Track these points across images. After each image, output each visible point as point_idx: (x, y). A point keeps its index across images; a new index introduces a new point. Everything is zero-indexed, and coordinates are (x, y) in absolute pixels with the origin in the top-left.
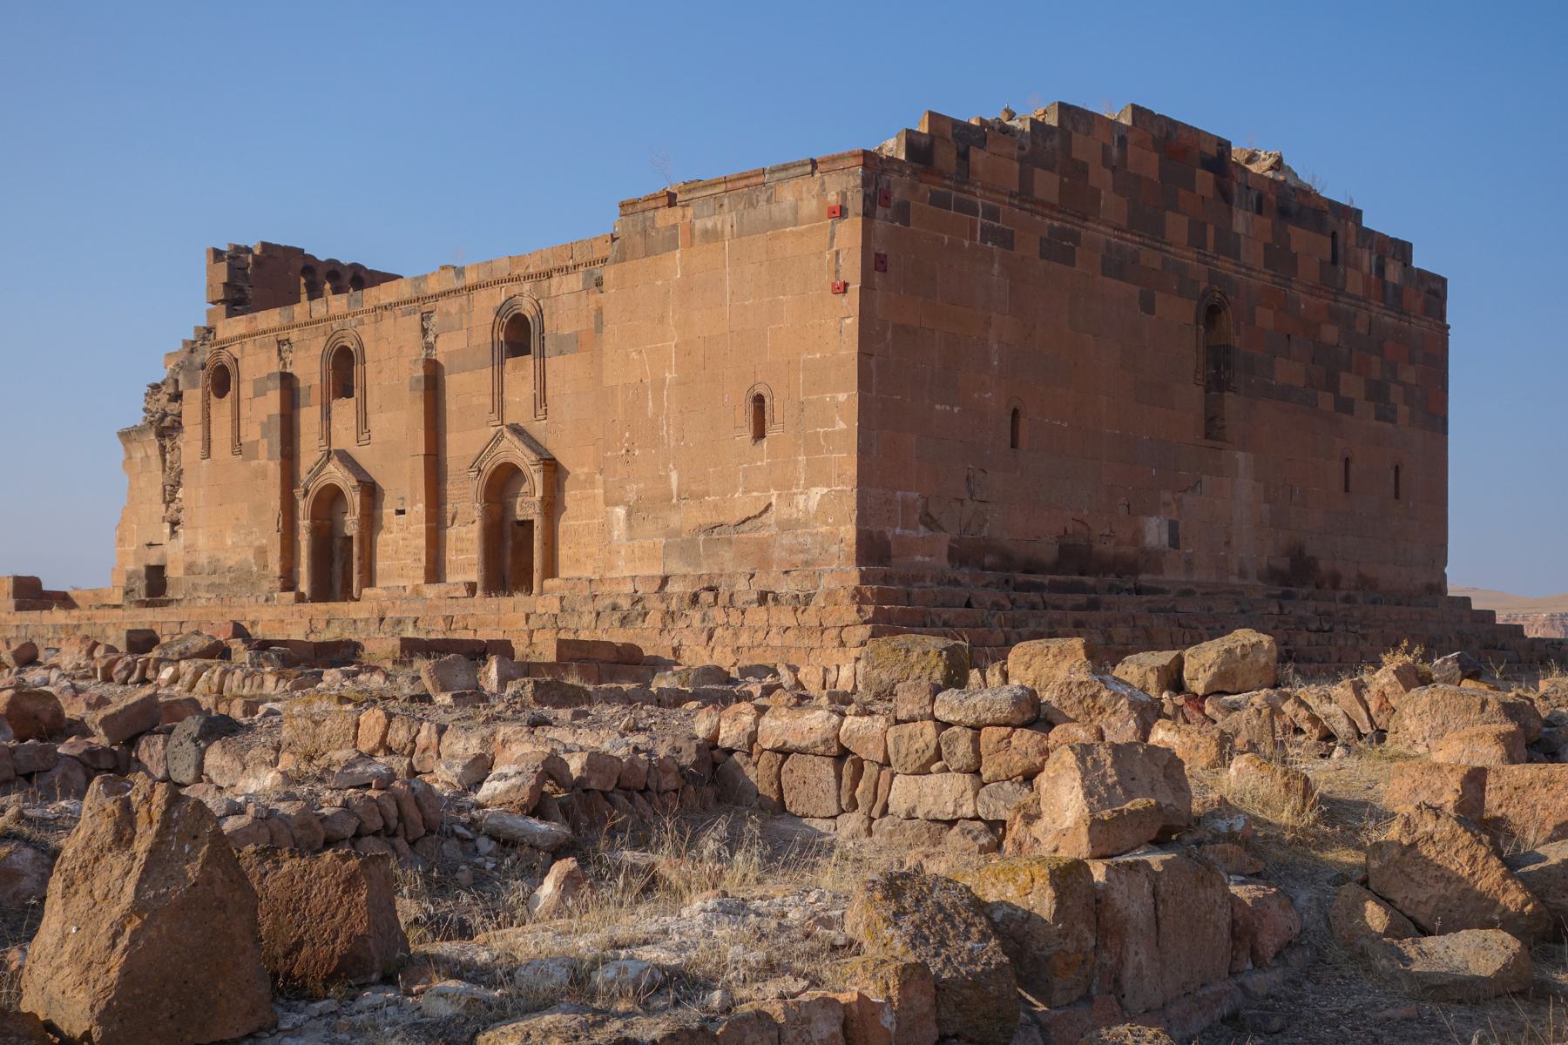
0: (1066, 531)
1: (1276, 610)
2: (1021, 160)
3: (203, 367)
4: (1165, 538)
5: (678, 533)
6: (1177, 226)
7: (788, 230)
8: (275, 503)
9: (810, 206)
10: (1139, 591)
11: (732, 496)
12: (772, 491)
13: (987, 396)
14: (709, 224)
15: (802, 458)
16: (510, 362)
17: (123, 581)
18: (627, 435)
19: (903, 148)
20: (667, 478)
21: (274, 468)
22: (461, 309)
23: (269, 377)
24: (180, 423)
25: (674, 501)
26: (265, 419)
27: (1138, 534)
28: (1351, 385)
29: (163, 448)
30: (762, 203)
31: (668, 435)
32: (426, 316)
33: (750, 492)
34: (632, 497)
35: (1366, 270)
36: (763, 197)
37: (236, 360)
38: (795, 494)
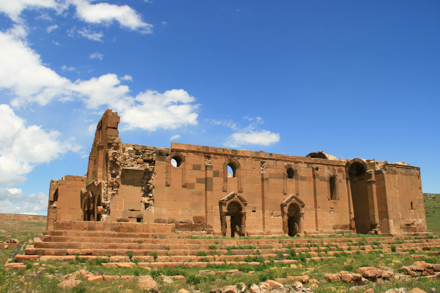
14: (402, 171)
15: (418, 214)
20: (399, 215)
34: (394, 218)
37: (185, 157)
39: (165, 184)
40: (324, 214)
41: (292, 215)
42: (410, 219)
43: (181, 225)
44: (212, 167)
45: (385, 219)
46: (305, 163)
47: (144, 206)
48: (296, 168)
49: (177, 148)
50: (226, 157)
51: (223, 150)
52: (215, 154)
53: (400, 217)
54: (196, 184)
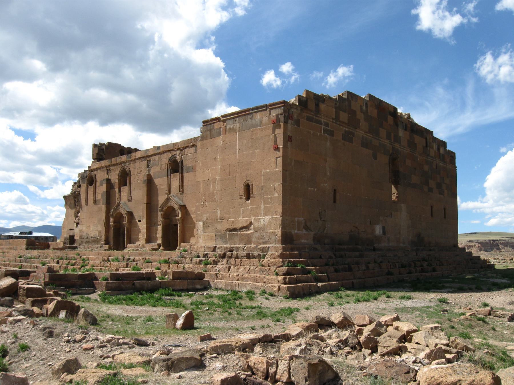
0: (351, 230)
1: (415, 254)
2: (336, 108)
3: (87, 177)
4: (381, 232)
5: (220, 231)
6: (383, 132)
7: (258, 128)
8: (104, 218)
9: (265, 120)
10: (374, 249)
11: (238, 219)
13: (326, 185)
14: (231, 127)
15: (262, 206)
16: (172, 175)
17: (63, 240)
18: (204, 198)
19: (297, 101)
20: (216, 212)
21: (103, 207)
23: (104, 180)
24: (80, 194)
26: (102, 192)
27: (374, 230)
28: (432, 184)
29: (75, 201)
32: (148, 162)
33: (244, 217)
34: (205, 218)
35: (435, 149)
42: (239, 217)
50: (121, 165)
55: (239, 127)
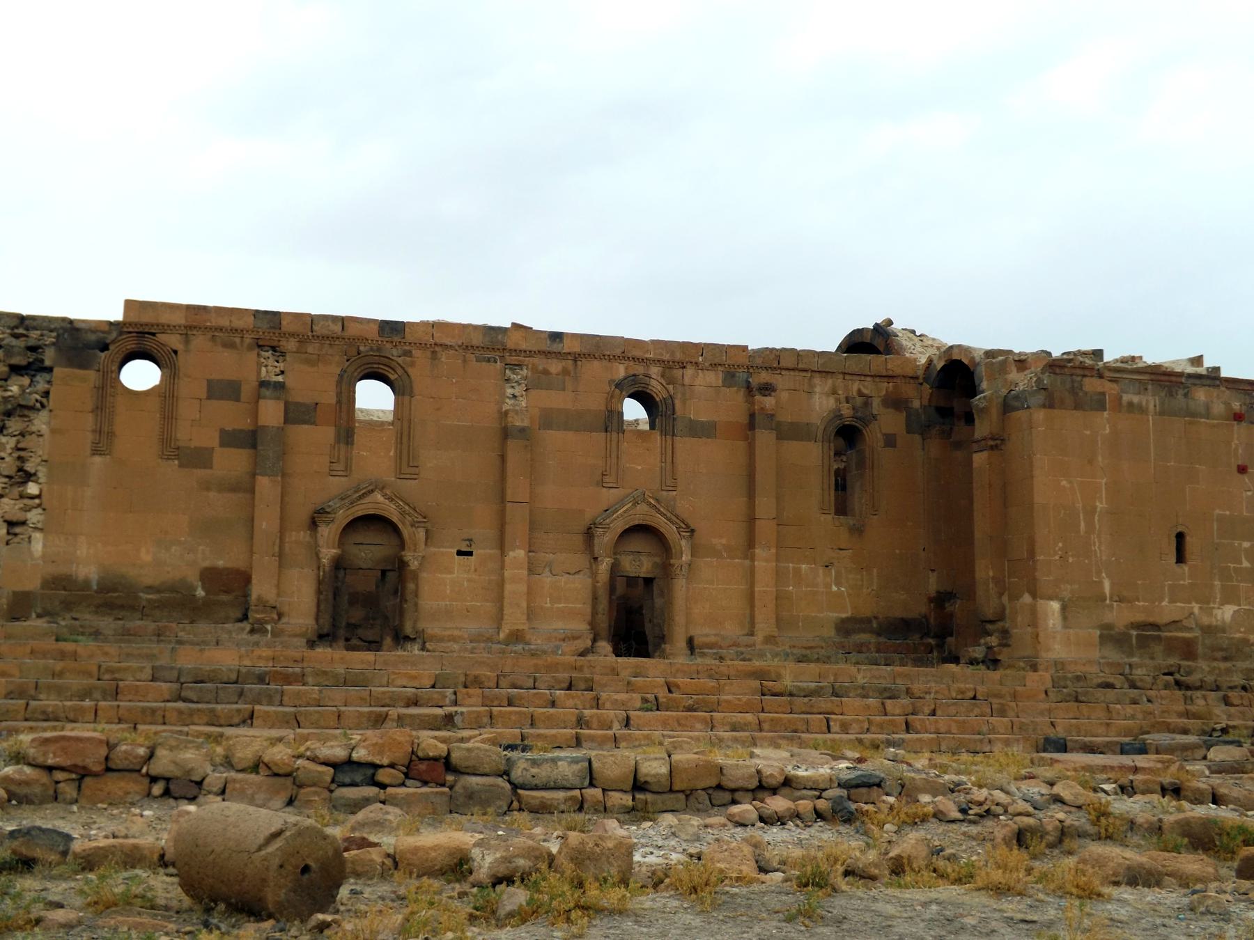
7: (1203, 420)
9: (1218, 408)
11: (1160, 603)
12: (1194, 604)
14: (1136, 399)
15: (1217, 583)
18: (1060, 545)
20: (1100, 583)
22: (565, 372)
25: (1108, 602)
30: (1180, 396)
31: (1100, 550)
33: (1176, 602)
34: (1066, 594)
36: (1181, 392)
38: (1213, 608)
39: (89, 452)
40: (797, 572)
41: (644, 569)
42: (1162, 599)
43: (149, 601)
44: (280, 386)
45: (1027, 598)
46: (714, 366)
47: (5, 531)
48: (671, 387)
49: (146, 318)
51: (340, 324)
52: (303, 340)
53: (1104, 593)
54: (218, 450)
55: (1155, 406)
